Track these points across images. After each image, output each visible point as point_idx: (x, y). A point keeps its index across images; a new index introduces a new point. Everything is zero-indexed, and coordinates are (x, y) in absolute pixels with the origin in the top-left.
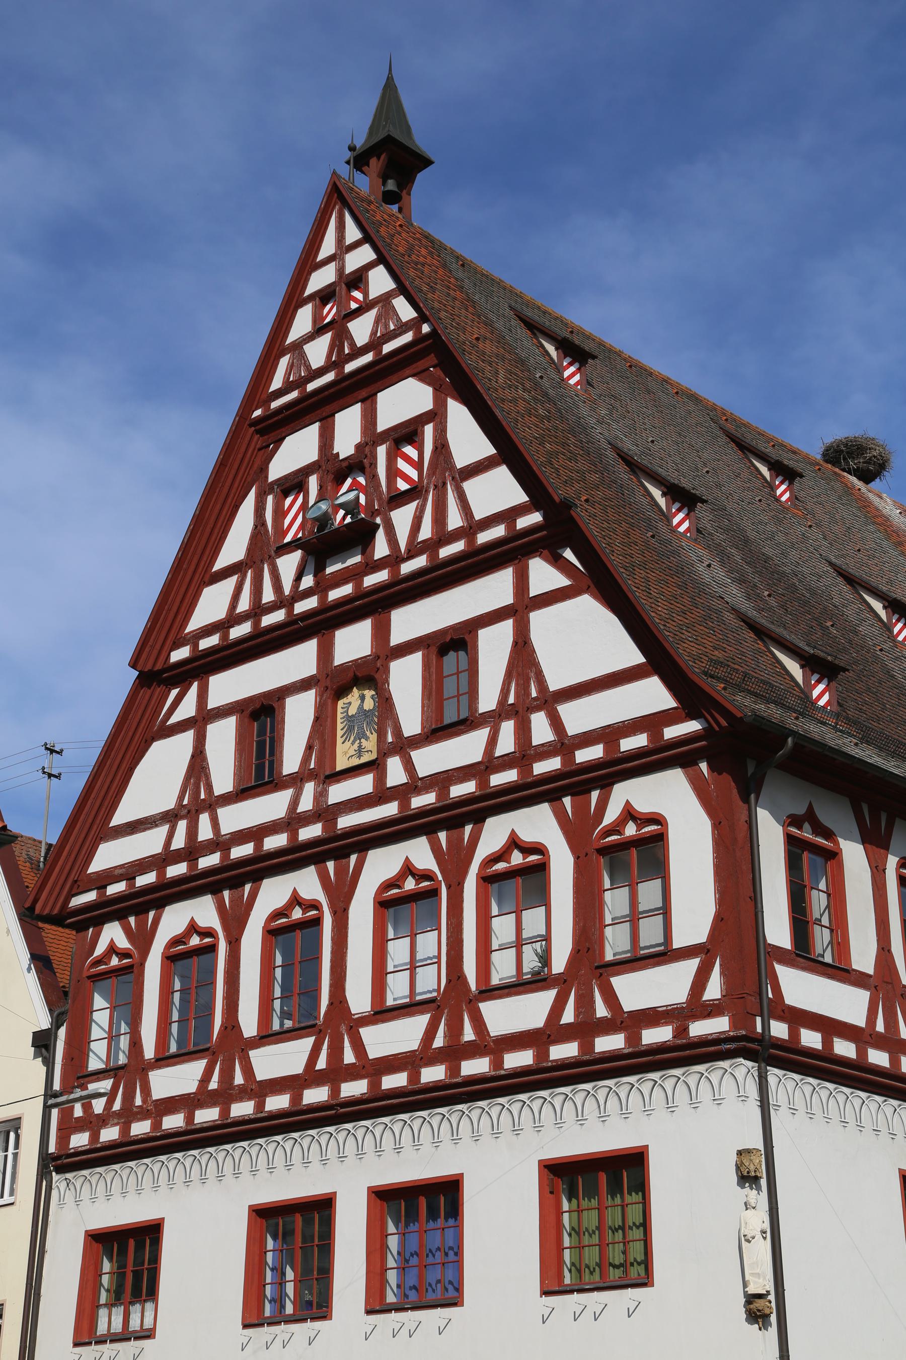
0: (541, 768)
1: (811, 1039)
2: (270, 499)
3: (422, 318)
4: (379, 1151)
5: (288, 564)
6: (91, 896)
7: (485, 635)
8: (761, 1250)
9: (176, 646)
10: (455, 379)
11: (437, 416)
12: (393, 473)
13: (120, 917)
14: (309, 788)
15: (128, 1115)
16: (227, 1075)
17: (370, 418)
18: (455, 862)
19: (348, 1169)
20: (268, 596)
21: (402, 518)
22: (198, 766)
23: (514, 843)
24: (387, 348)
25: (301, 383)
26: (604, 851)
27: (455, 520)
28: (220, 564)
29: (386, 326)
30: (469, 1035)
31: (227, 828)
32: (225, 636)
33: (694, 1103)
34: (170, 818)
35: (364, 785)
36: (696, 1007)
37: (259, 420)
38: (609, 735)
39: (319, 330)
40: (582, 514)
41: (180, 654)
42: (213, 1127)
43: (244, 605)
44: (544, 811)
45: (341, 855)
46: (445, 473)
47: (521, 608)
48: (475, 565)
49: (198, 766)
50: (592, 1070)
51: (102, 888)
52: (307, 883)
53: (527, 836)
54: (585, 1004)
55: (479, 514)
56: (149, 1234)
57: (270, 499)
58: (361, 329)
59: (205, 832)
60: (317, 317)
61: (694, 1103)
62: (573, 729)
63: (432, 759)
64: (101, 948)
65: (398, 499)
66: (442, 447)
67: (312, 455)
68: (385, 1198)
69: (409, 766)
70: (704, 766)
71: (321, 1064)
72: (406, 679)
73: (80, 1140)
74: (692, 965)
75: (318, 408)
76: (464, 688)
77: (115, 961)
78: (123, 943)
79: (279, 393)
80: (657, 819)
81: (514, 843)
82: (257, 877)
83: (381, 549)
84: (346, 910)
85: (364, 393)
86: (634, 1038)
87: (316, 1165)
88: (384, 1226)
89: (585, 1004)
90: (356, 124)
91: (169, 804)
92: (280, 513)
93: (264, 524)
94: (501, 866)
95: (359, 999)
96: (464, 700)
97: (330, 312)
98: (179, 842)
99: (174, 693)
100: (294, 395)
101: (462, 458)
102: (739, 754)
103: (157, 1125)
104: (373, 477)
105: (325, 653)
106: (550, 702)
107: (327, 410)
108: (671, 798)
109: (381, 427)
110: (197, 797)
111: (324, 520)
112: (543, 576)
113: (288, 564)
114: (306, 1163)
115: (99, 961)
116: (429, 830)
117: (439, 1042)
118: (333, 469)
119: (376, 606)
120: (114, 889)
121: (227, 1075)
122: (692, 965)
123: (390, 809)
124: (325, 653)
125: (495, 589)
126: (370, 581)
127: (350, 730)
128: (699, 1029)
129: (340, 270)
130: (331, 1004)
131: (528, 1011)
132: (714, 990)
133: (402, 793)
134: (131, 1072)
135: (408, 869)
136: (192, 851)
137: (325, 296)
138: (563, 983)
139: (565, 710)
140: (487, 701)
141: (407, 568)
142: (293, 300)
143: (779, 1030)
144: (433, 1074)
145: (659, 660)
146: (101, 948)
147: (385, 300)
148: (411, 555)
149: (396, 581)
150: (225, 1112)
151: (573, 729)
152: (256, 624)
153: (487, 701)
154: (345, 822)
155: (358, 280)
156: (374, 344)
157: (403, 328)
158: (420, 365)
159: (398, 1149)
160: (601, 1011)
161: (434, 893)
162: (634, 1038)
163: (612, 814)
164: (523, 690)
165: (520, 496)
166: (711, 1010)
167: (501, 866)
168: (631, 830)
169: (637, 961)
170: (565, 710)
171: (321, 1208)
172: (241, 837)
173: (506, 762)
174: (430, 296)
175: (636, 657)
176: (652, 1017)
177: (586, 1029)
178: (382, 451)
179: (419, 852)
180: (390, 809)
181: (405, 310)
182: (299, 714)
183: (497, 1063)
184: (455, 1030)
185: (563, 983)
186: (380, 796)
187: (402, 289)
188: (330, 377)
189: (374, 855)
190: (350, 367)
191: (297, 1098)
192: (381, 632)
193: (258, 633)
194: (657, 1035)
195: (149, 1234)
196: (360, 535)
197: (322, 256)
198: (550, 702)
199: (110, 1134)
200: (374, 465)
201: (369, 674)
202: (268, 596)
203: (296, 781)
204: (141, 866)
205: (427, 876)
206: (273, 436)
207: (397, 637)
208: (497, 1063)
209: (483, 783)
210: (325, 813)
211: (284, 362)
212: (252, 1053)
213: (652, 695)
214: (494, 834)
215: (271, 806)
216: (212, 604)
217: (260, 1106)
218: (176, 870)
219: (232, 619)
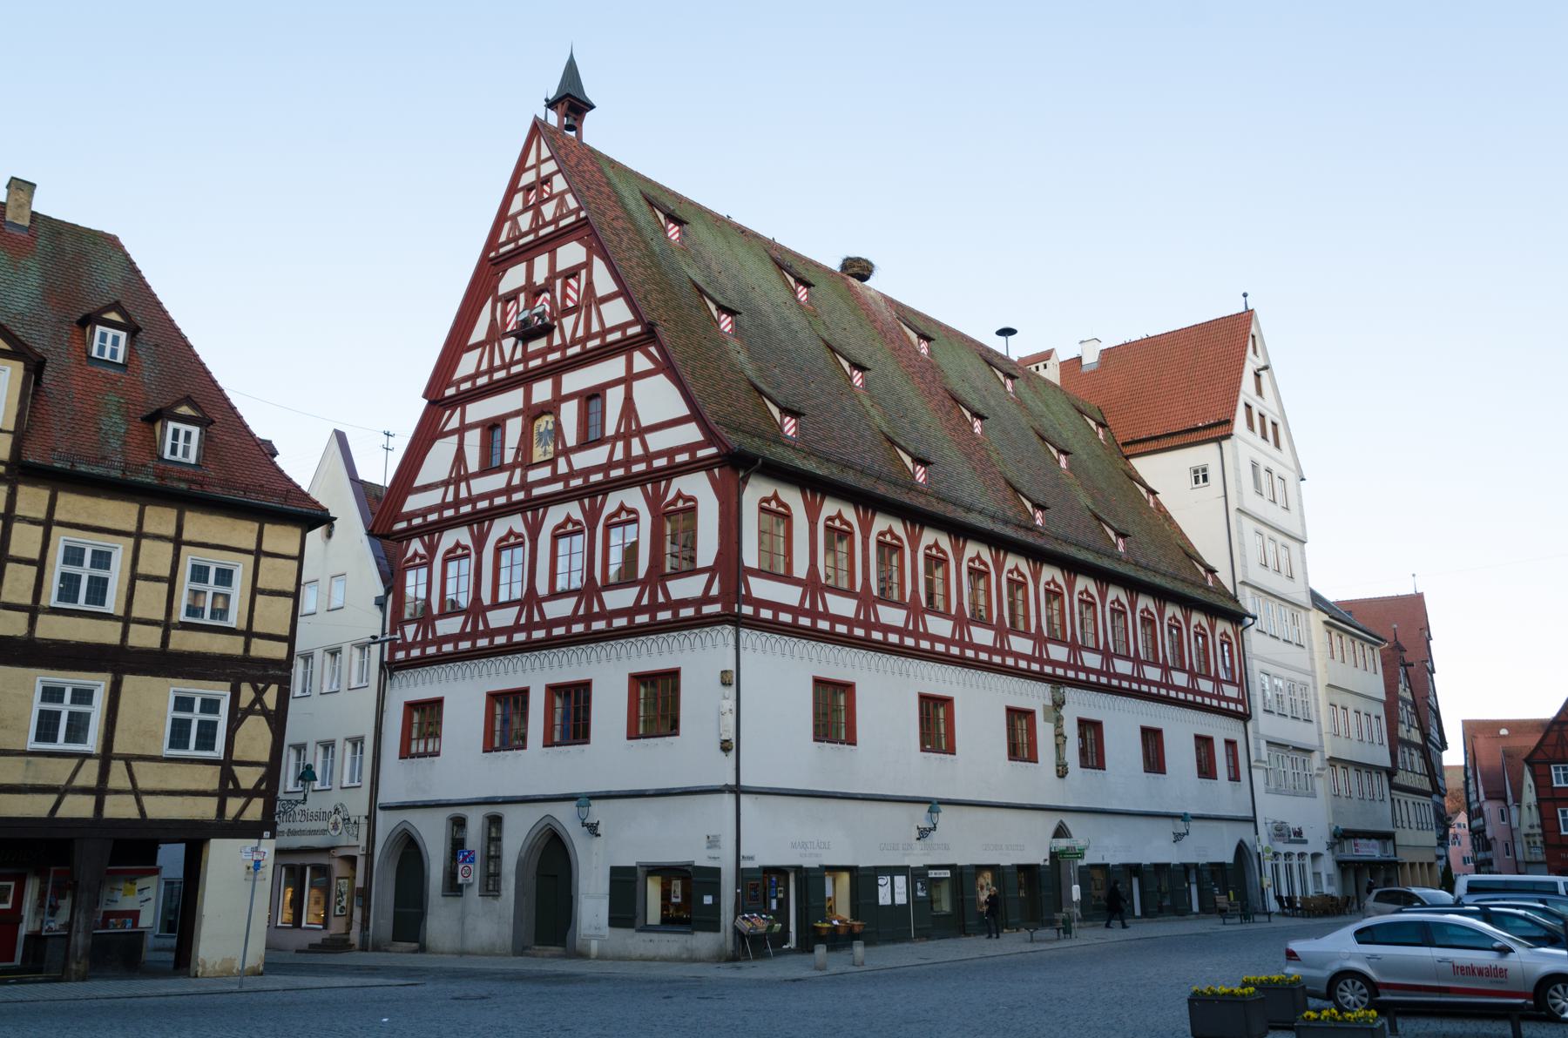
1: (766, 614)
3: (580, 209)
4: (551, 666)
5: (508, 343)
7: (609, 392)
8: (731, 719)
9: (448, 386)
10: (597, 247)
11: (588, 265)
12: (565, 296)
13: (420, 536)
14: (518, 472)
15: (425, 643)
16: (475, 625)
18: (592, 515)
19: (536, 675)
20: (497, 362)
21: (568, 322)
22: (460, 457)
23: (622, 508)
24: (562, 223)
25: (515, 239)
27: (595, 328)
28: (473, 340)
30: (596, 609)
31: (475, 492)
33: (703, 646)
35: (545, 472)
36: (706, 599)
38: (670, 453)
39: (526, 209)
40: (659, 329)
41: (450, 392)
42: (468, 651)
43: (484, 366)
44: (637, 491)
46: (591, 299)
47: (629, 379)
48: (605, 353)
49: (460, 457)
51: (409, 521)
53: (628, 505)
54: (653, 596)
55: (608, 325)
56: (438, 703)
58: (548, 211)
59: (463, 493)
60: (526, 201)
61: (703, 646)
62: (652, 448)
63: (582, 460)
64: (410, 554)
65: (567, 312)
66: (590, 284)
67: (521, 282)
68: (553, 690)
71: (523, 621)
72: (569, 413)
73: (400, 655)
74: (706, 576)
75: (525, 254)
78: (421, 551)
79: (504, 244)
80: (692, 499)
81: (622, 508)
83: (557, 341)
86: (675, 614)
87: (520, 673)
88: (553, 702)
89: (653, 596)
91: (445, 476)
94: (616, 520)
98: (450, 498)
101: (600, 293)
102: (734, 466)
103: (439, 649)
104: (553, 297)
105: (528, 396)
106: (642, 432)
107: (530, 254)
109: (559, 268)
112: (641, 362)
113: (508, 343)
114: (515, 672)
115: (409, 560)
116: (580, 498)
117: (581, 612)
118: (533, 291)
120: (417, 521)
121: (475, 625)
122: (706, 576)
124: (528, 396)
125: (614, 368)
126: (551, 357)
128: (707, 610)
129: (538, 174)
132: (715, 591)
133: (566, 478)
134: (425, 618)
135: (569, 519)
136: (457, 503)
138: (643, 584)
139: (648, 437)
140: (610, 430)
141: (571, 352)
142: (512, 190)
143: (747, 610)
144: (578, 628)
145: (696, 415)
146: (410, 554)
147: (562, 194)
149: (564, 359)
150: (474, 644)
151: (652, 448)
153: (610, 430)
154: (536, 492)
155: (547, 180)
156: (555, 221)
157: (571, 213)
158: (580, 233)
159: (561, 666)
160: (661, 599)
162: (675, 614)
163: (671, 495)
164: (628, 426)
165: (629, 317)
167: (616, 520)
168: (680, 504)
169: (678, 574)
170: (648, 437)
171: (524, 692)
172: (482, 497)
173: (618, 465)
176: (685, 603)
177: (653, 608)
178: (559, 283)
179: (574, 510)
180: (559, 486)
181: (572, 203)
183: (609, 624)
184: (589, 606)
185: (643, 584)
187: (570, 189)
188: (531, 237)
189: (552, 510)
190: (542, 233)
191: (510, 638)
192: (557, 387)
193: (491, 383)
194: (687, 612)
195: (438, 703)
196: (547, 330)
198: (642, 432)
199: (415, 653)
202: (497, 362)
204: (431, 510)
205: (577, 523)
206: (502, 266)
207: (565, 391)
208: (609, 624)
209: (607, 475)
210: (526, 486)
211: (507, 225)
213: (691, 433)
214: (612, 502)
215: (498, 481)
216: (468, 364)
217: (491, 642)
218: (449, 513)
219: (478, 374)
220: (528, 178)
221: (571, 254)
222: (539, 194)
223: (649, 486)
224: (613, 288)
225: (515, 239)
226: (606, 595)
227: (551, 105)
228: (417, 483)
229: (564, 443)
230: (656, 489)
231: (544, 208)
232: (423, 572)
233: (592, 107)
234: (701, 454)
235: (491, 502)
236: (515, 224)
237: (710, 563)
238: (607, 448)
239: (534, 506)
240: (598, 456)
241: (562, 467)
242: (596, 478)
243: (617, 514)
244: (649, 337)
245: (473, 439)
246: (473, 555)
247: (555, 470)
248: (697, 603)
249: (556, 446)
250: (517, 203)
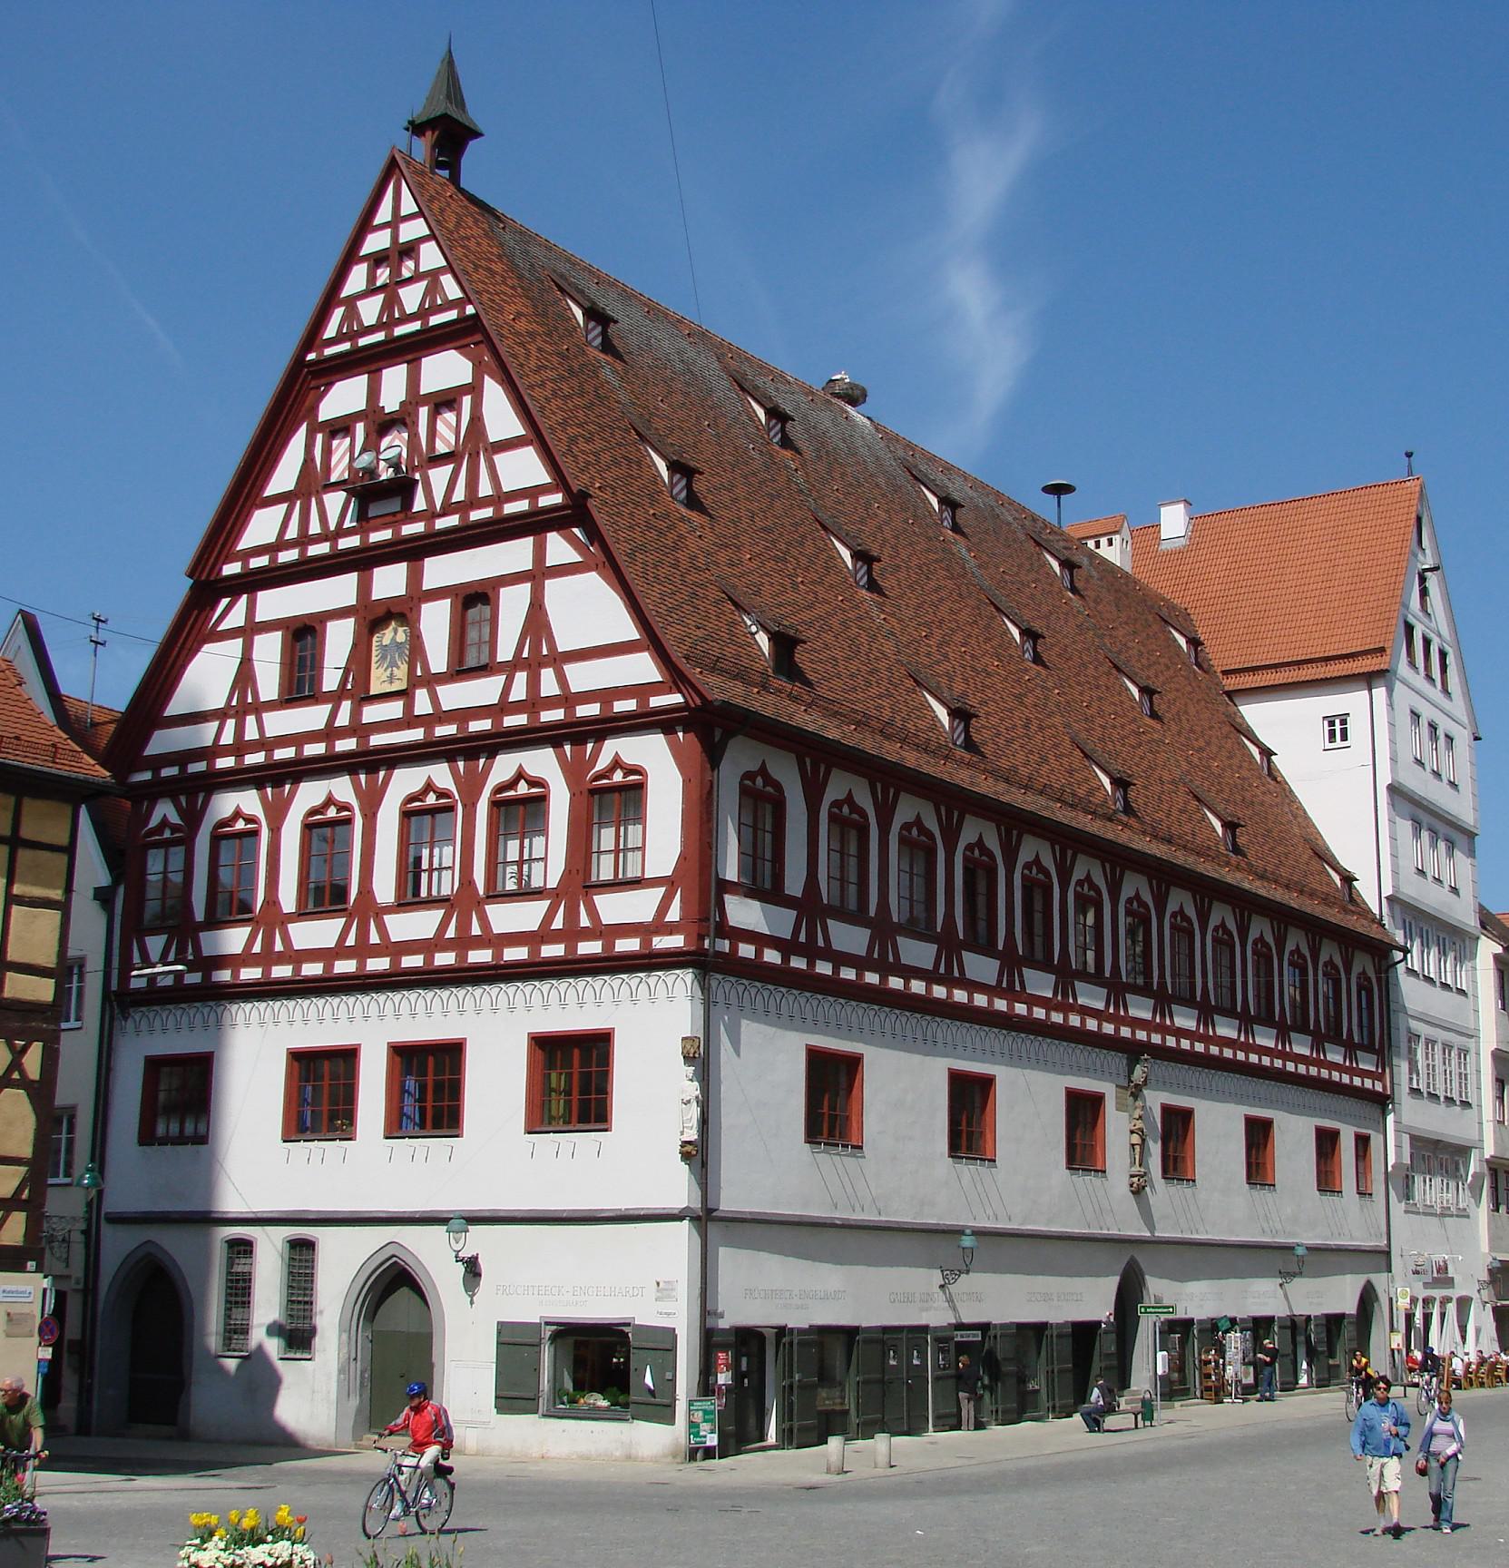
2: (320, 437)
3: (467, 300)
5: (335, 501)
6: (147, 776)
7: (505, 593)
9: (228, 560)
11: (475, 389)
14: (346, 705)
17: (414, 380)
21: (439, 477)
22: (245, 675)
24: (435, 320)
26: (593, 792)
27: (485, 489)
28: (271, 490)
29: (433, 300)
30: (476, 930)
32: (273, 559)
34: (221, 715)
35: (394, 710)
37: (313, 363)
41: (232, 569)
43: (292, 533)
44: (549, 752)
45: (372, 769)
47: (538, 575)
49: (245, 675)
51: (156, 771)
52: (342, 788)
53: (532, 771)
54: (572, 915)
55: (507, 487)
57: (320, 437)
58: (411, 297)
59: (251, 733)
60: (372, 277)
62: (576, 687)
63: (455, 696)
64: (155, 821)
66: (477, 418)
67: (361, 405)
72: (436, 621)
74: (660, 892)
75: (368, 362)
76: (487, 638)
77: (167, 834)
78: (174, 818)
81: (520, 775)
82: (297, 779)
83: (419, 504)
84: (375, 815)
85: (410, 357)
86: (609, 945)
89: (572, 915)
90: (418, 100)
92: (328, 452)
93: (313, 460)
95: (385, 891)
96: (486, 649)
97: (383, 275)
99: (225, 601)
100: (346, 346)
101: (494, 435)
104: (414, 436)
105: (365, 588)
106: (559, 660)
108: (653, 757)
110: (244, 702)
111: (371, 472)
112: (559, 549)
113: (335, 501)
116: (450, 757)
117: (451, 933)
118: (381, 424)
119: (413, 552)
120: (168, 772)
122: (660, 892)
124: (365, 588)
125: (515, 554)
126: (408, 530)
127: (383, 658)
129: (395, 237)
130: (360, 892)
131: (527, 916)
137: (378, 259)
138: (555, 895)
140: (505, 653)
145: (652, 640)
146: (155, 821)
147: (434, 275)
148: (444, 514)
152: (303, 552)
153: (505, 653)
154: (377, 740)
155: (410, 250)
156: (422, 314)
157: (449, 305)
160: (585, 922)
161: (450, 809)
162: (609, 945)
163: (603, 763)
164: (536, 648)
165: (544, 478)
166: (671, 929)
168: (618, 777)
170: (569, 669)
172: (283, 741)
173: (517, 707)
174: (475, 276)
175: (633, 633)
177: (572, 934)
178: (424, 412)
179: (441, 774)
180: (417, 734)
181: (452, 290)
182: (339, 640)
185: (555, 895)
186: (409, 721)
187: (450, 268)
188: (380, 336)
189: (399, 773)
190: (400, 331)
192: (415, 578)
196: (402, 488)
197: (378, 221)
198: (559, 660)
200: (416, 423)
201: (402, 611)
202: (315, 528)
203: (336, 698)
205: (442, 794)
206: (323, 381)
207: (428, 584)
210: (359, 729)
211: (338, 313)
212: (290, 926)
213: (643, 668)
214: (504, 767)
215: (312, 717)
216: (262, 527)
219: (281, 544)
220: (376, 242)
221: (446, 369)
222: (396, 271)
223: (567, 748)
224: (516, 428)
225: (352, 336)
226: (492, 910)
227: (417, 129)
228: (172, 709)
231: (403, 292)
232: (178, 854)
233: (477, 135)
235: (299, 751)
236: (352, 314)
237: (667, 869)
239: (372, 763)
240: (485, 691)
241: (422, 704)
242: (477, 726)
243: (512, 784)
244: (574, 514)
245: (269, 649)
246: (265, 834)
247: (409, 707)
249: (412, 670)
250: (357, 279)
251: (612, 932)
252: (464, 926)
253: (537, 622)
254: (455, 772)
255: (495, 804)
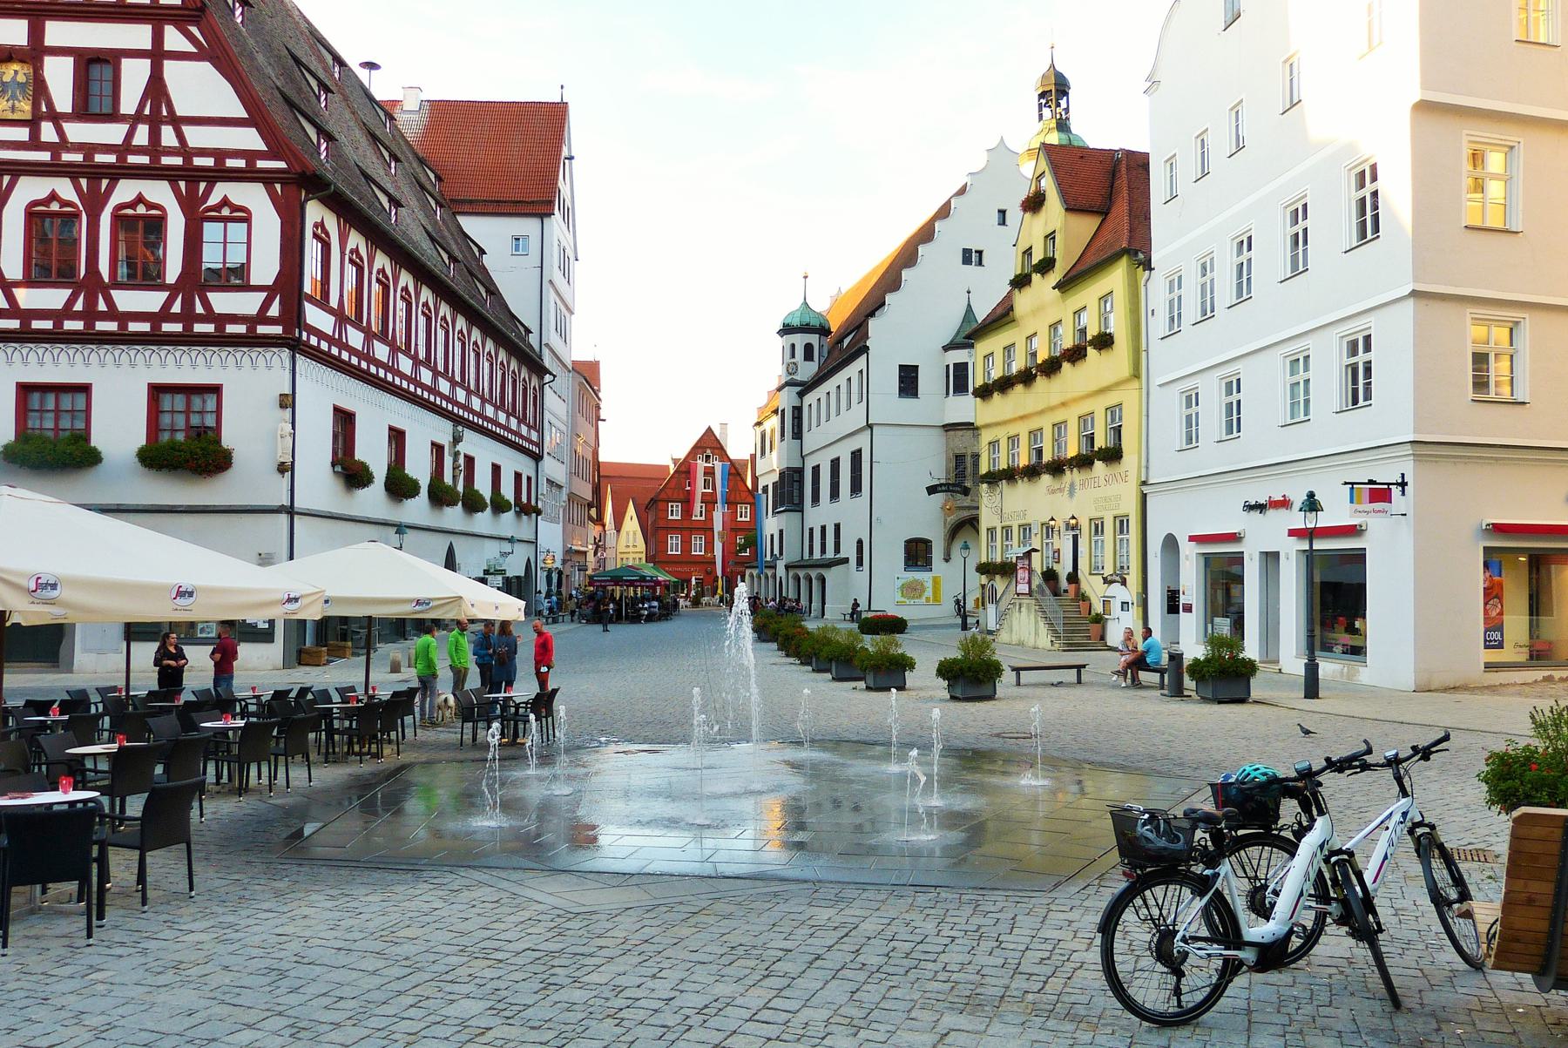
0: (166, 161)
7: (126, 64)
23: (140, 199)
35: (22, 134)
47: (157, 55)
50: (188, 339)
53: (151, 197)
54: (188, 305)
69: (60, 132)
70: (278, 187)
72: (59, 76)
81: (140, 199)
94: (129, 212)
112: (174, 39)
123: (45, 156)
125: (138, 36)
128: (262, 329)
132: (274, 311)
133: (56, 149)
135: (54, 196)
145: (255, 117)
151: (192, 143)
153: (128, 105)
160: (199, 309)
161: (77, 215)
163: (213, 200)
164: (156, 109)
167: (129, 212)
168: (226, 212)
170: (187, 130)
173: (140, 150)
175: (240, 112)
176: (234, 319)
180: (45, 156)
185: (174, 290)
186: (35, 143)
198: (177, 122)
214: (125, 191)
229: (50, 104)
230: (192, 188)
234: (261, 164)
238: (123, 128)
242: (100, 158)
243: (132, 205)
248: (251, 321)
251: (223, 320)
252: (91, 303)
253: (156, 88)
254: (78, 189)
255: (117, 218)
